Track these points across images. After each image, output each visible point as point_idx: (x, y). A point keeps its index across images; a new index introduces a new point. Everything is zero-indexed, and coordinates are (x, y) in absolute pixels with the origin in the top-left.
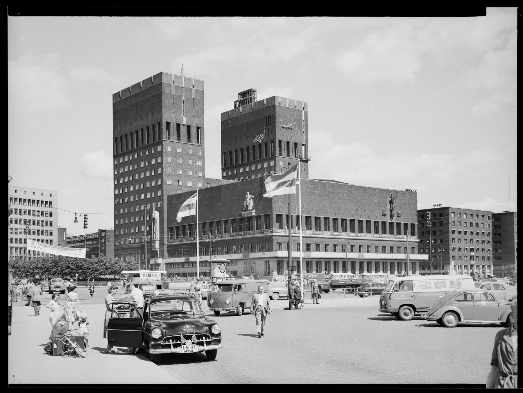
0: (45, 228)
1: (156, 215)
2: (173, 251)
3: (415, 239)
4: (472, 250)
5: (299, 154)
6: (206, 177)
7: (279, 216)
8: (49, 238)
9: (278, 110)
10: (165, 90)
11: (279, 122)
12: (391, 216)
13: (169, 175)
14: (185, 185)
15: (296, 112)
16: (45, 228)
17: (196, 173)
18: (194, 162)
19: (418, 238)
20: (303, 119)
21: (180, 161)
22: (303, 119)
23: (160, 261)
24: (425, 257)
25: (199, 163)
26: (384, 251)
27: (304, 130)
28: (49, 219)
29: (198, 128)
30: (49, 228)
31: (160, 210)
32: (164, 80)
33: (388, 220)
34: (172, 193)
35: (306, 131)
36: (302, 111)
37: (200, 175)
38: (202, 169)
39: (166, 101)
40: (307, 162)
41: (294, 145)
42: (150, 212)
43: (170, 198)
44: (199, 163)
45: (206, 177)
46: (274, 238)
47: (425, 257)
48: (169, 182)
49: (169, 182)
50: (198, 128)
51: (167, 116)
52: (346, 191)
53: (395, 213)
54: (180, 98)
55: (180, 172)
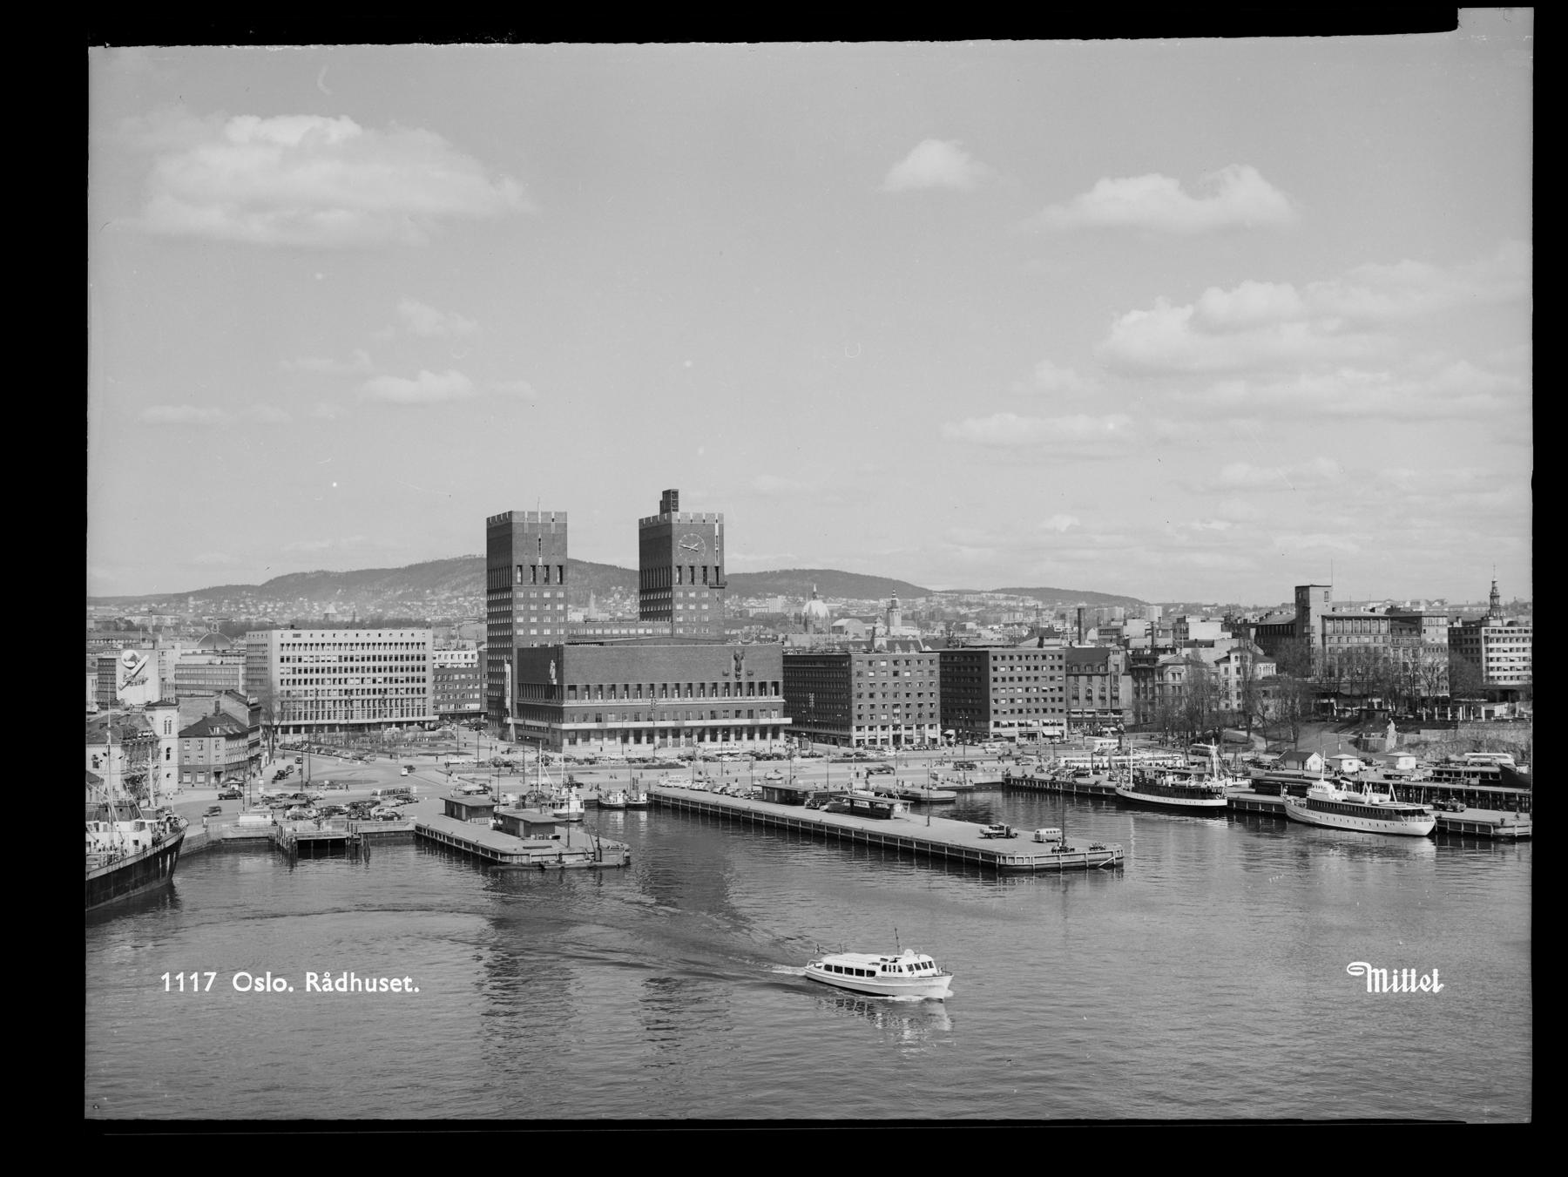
0: (416, 674)
1: (508, 668)
2: (524, 710)
3: (780, 699)
4: (896, 706)
7: (573, 688)
8: (421, 685)
10: (516, 530)
11: (678, 544)
13: (520, 626)
14: (540, 634)
16: (416, 674)
18: (554, 607)
21: (533, 608)
23: (510, 720)
24: (789, 721)
26: (714, 717)
28: (421, 663)
30: (421, 674)
31: (509, 662)
32: (515, 519)
33: (733, 680)
34: (524, 645)
35: (722, 549)
39: (517, 542)
42: (501, 663)
43: (521, 651)
47: (789, 721)
48: (520, 632)
49: (520, 632)
51: (516, 560)
55: (534, 620)
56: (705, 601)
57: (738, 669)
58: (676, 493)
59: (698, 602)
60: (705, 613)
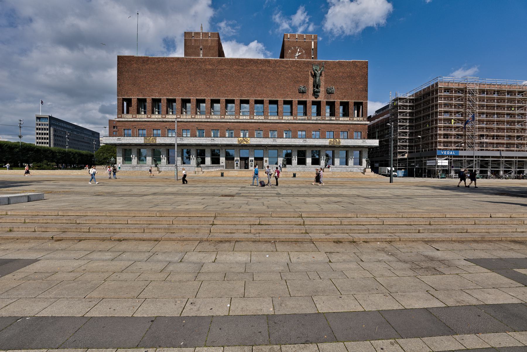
15: (305, 43)
20: (313, 47)
22: (313, 47)
53: (322, 89)
57: (316, 86)
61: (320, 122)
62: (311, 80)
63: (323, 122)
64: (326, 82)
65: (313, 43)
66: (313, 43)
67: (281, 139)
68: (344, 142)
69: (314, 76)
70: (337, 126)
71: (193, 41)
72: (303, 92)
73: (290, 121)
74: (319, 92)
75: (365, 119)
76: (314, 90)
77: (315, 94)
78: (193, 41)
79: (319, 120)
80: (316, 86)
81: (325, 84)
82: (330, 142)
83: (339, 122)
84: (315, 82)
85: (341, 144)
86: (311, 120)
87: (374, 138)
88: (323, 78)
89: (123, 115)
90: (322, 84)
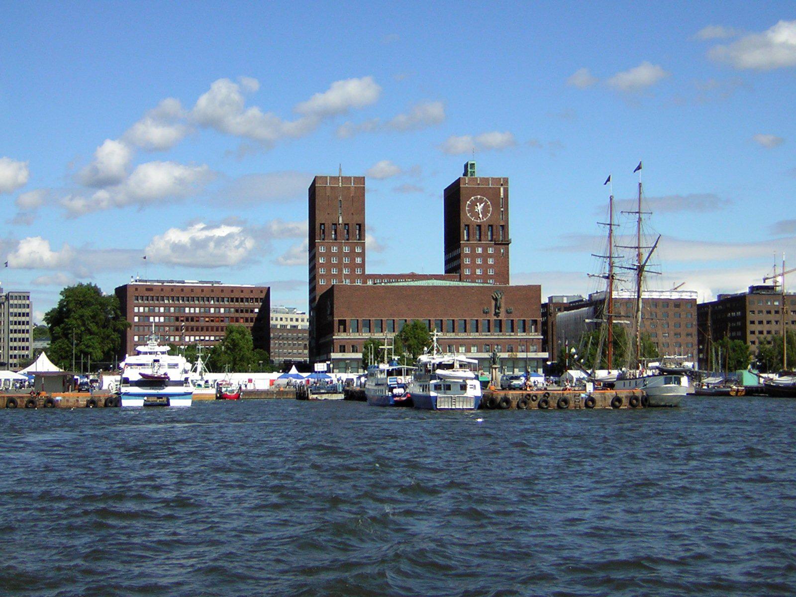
5: (494, 237)
6: (367, 273)
9: (462, 192)
12: (497, 314)
15: (490, 190)
17: (353, 270)
19: (542, 335)
25: (358, 260)
27: (502, 209)
29: (360, 225)
36: (500, 188)
37: (358, 272)
38: (362, 266)
40: (508, 244)
41: (487, 227)
44: (358, 260)
45: (367, 273)
46: (335, 341)
50: (360, 225)
52: (430, 292)
53: (502, 310)
54: (337, 198)
55: (334, 271)
56: (490, 256)
57: (497, 307)
58: (472, 165)
59: (485, 256)
60: (491, 266)
61: (501, 337)
62: (493, 303)
63: (503, 337)
64: (506, 303)
65: (502, 189)
66: (502, 189)
67: (470, 354)
68: (521, 355)
69: (496, 300)
70: (516, 340)
71: (329, 189)
72: (487, 313)
73: (477, 337)
74: (499, 313)
75: (540, 334)
76: (495, 311)
77: (497, 314)
78: (329, 189)
79: (501, 335)
80: (497, 307)
81: (505, 305)
82: (509, 355)
83: (517, 337)
84: (496, 305)
85: (518, 357)
86: (494, 335)
87: (546, 352)
88: (503, 300)
89: (339, 334)
90: (503, 305)
